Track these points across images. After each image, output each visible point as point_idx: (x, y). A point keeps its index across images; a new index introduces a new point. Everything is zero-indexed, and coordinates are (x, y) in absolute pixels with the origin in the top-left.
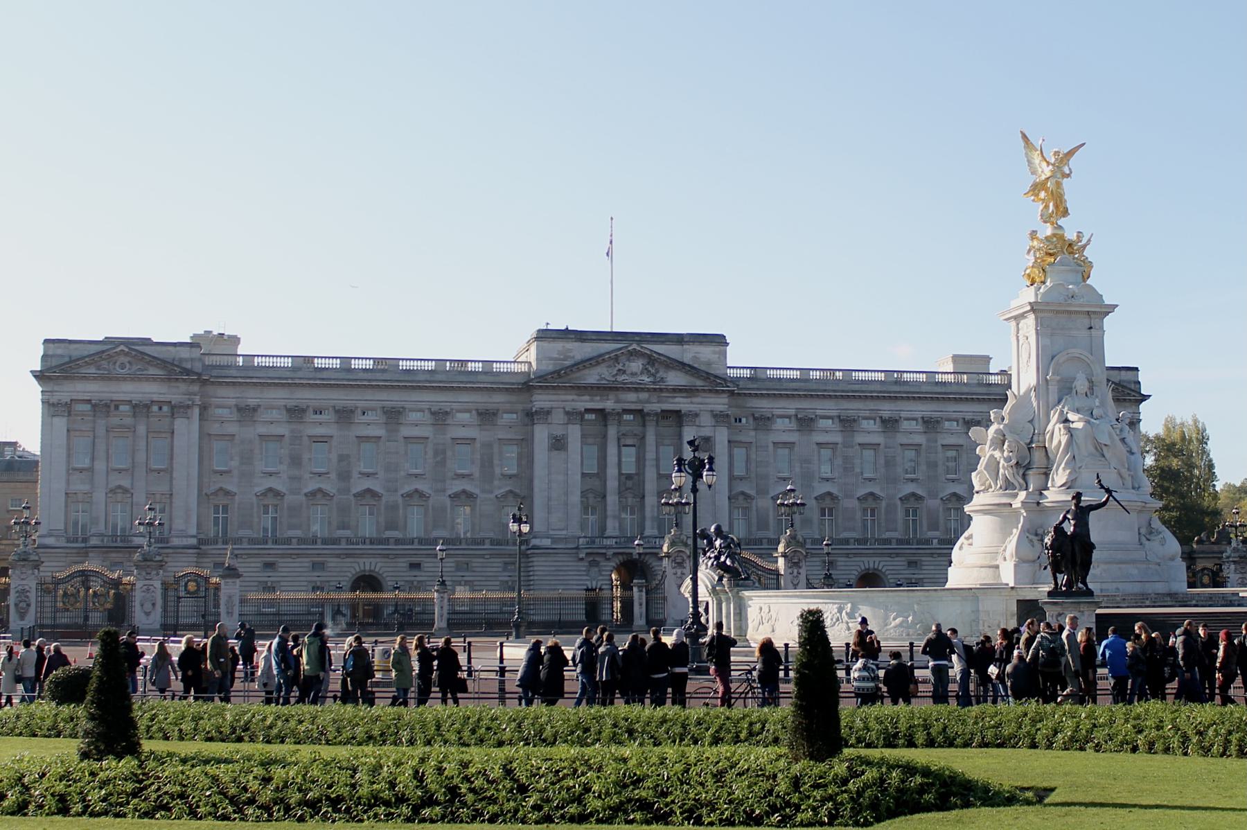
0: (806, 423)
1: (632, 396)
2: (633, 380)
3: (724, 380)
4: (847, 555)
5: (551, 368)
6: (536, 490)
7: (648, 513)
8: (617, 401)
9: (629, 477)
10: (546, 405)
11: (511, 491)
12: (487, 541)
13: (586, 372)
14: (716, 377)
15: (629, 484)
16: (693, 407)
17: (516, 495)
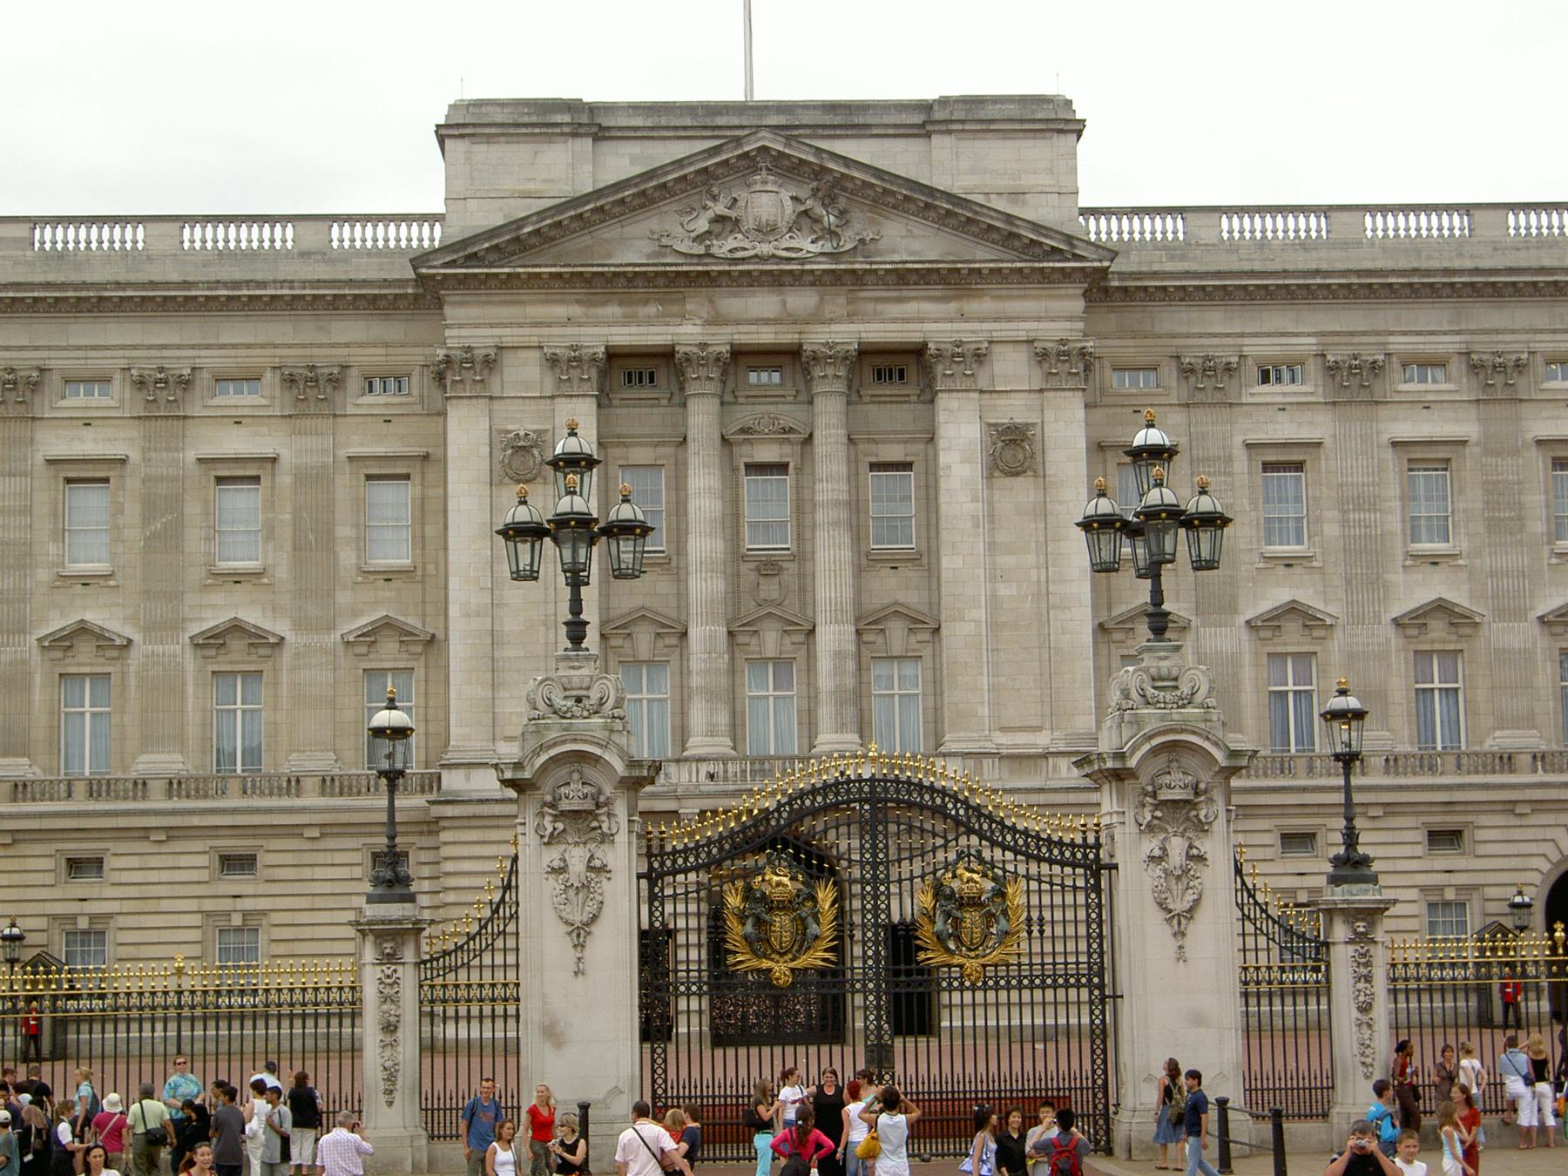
0: (1355, 380)
1: (763, 303)
2: (765, 249)
3: (1069, 239)
4: (1510, 807)
5: (498, 220)
6: (454, 611)
7: (825, 682)
8: (717, 320)
9: (769, 567)
10: (482, 339)
11: (387, 625)
12: (310, 784)
13: (609, 232)
14: (1035, 226)
15: (770, 589)
16: (971, 332)
17: (404, 634)
